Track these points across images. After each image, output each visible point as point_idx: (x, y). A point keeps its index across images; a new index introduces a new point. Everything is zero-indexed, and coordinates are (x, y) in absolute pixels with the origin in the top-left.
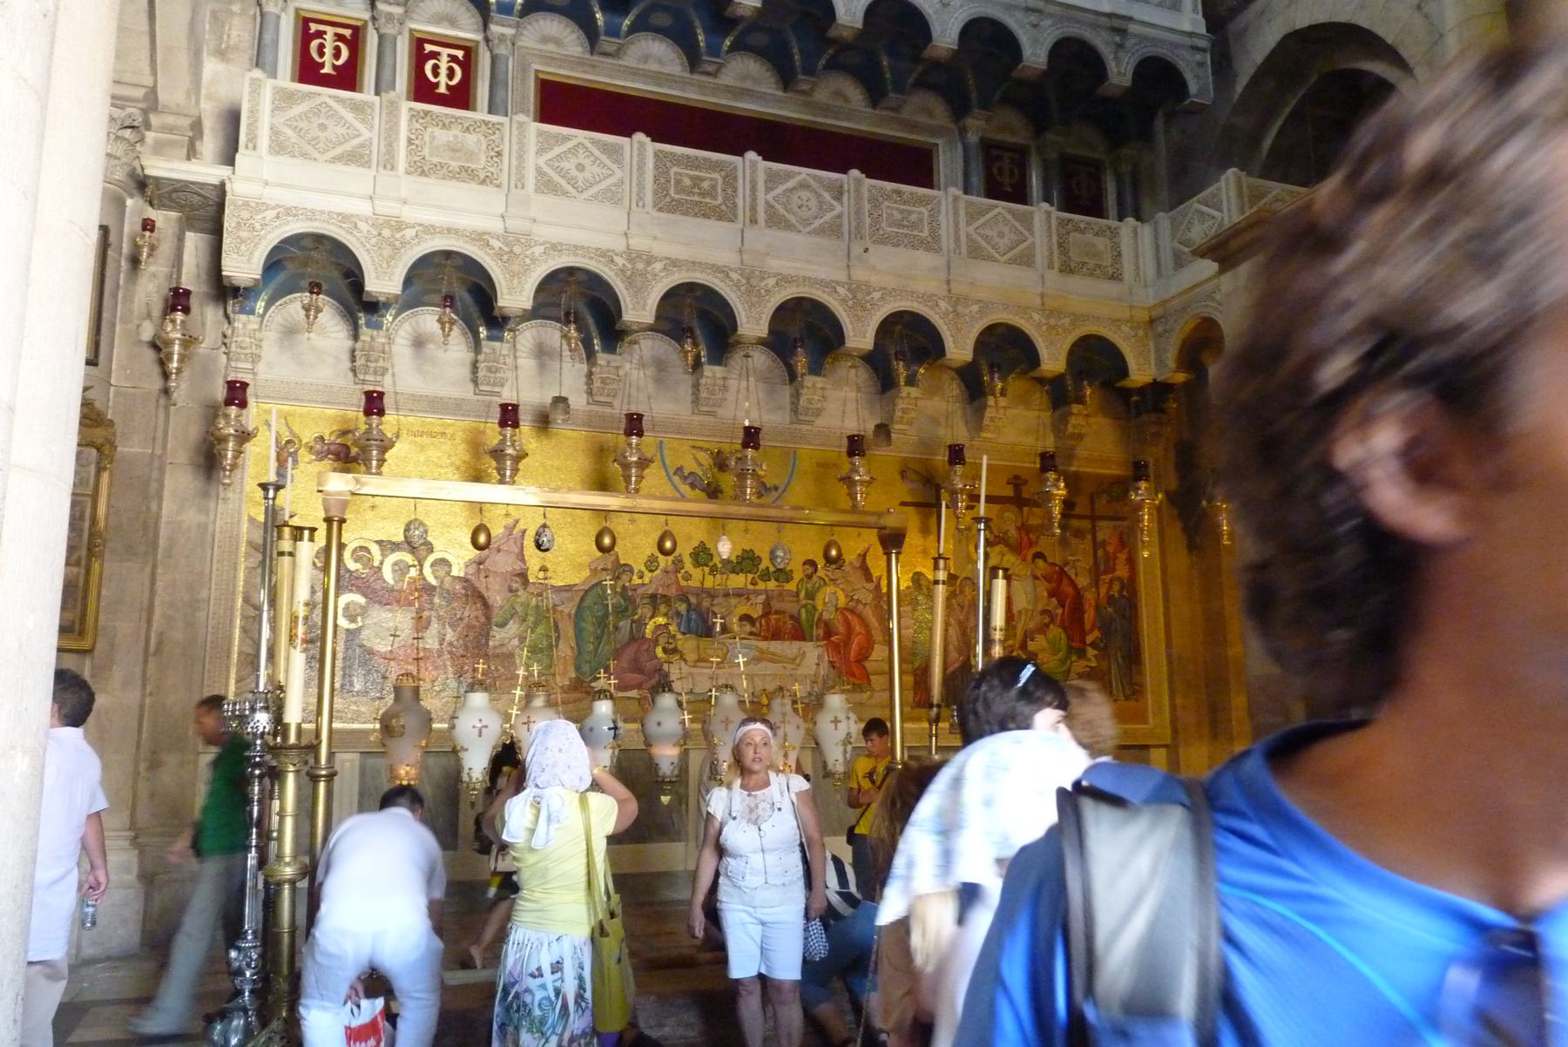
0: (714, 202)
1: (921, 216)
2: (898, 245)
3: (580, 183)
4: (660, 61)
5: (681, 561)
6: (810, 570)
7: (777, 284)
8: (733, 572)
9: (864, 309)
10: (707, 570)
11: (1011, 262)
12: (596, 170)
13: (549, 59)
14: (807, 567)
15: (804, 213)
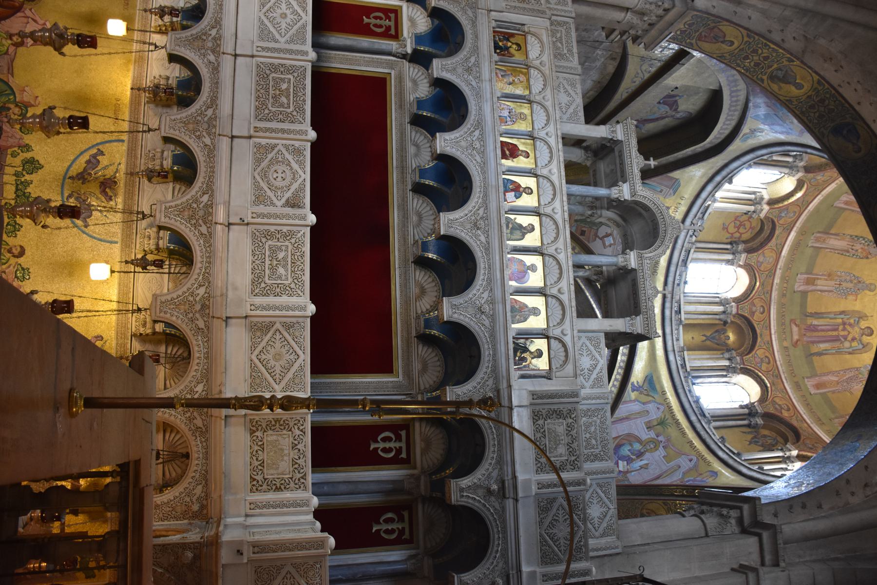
0: (270, 105)
1: (283, 277)
2: (254, 255)
3: (271, 15)
4: (416, 155)
5: (28, 151)
6: (16, 251)
7: (206, 145)
8: (17, 190)
9: (191, 218)
10: (20, 169)
11: (253, 367)
12: (284, 26)
13: (400, 79)
14: (19, 249)
15: (271, 175)
